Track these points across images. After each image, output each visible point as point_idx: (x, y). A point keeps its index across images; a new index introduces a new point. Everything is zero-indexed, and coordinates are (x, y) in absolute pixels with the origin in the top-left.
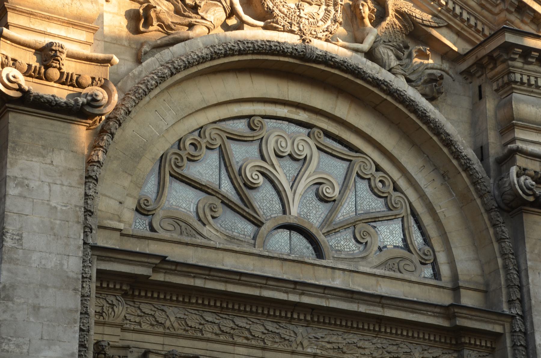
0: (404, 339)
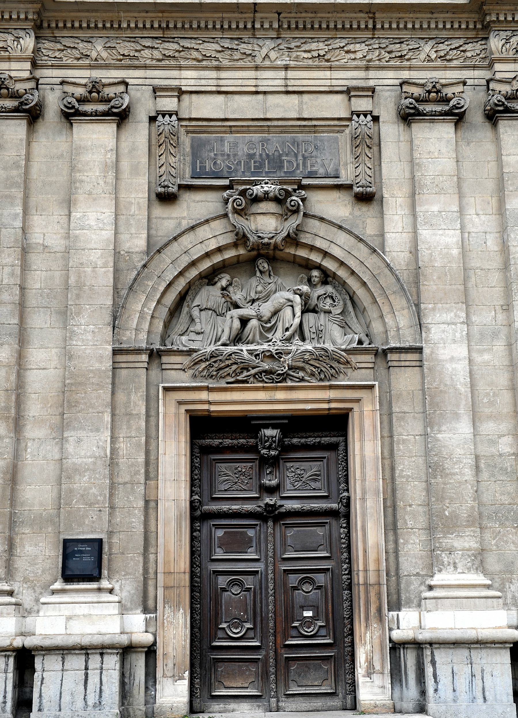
0: (411, 35)
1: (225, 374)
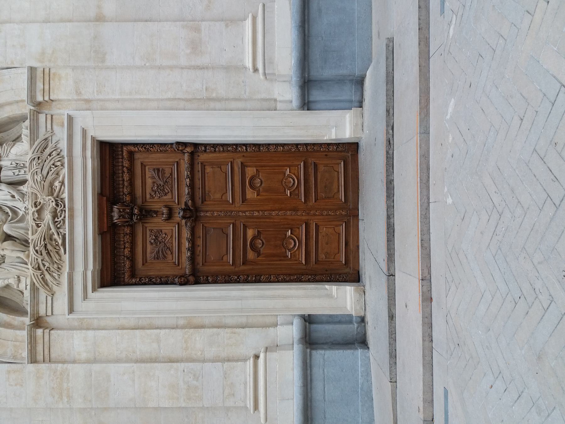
1: (57, 255)
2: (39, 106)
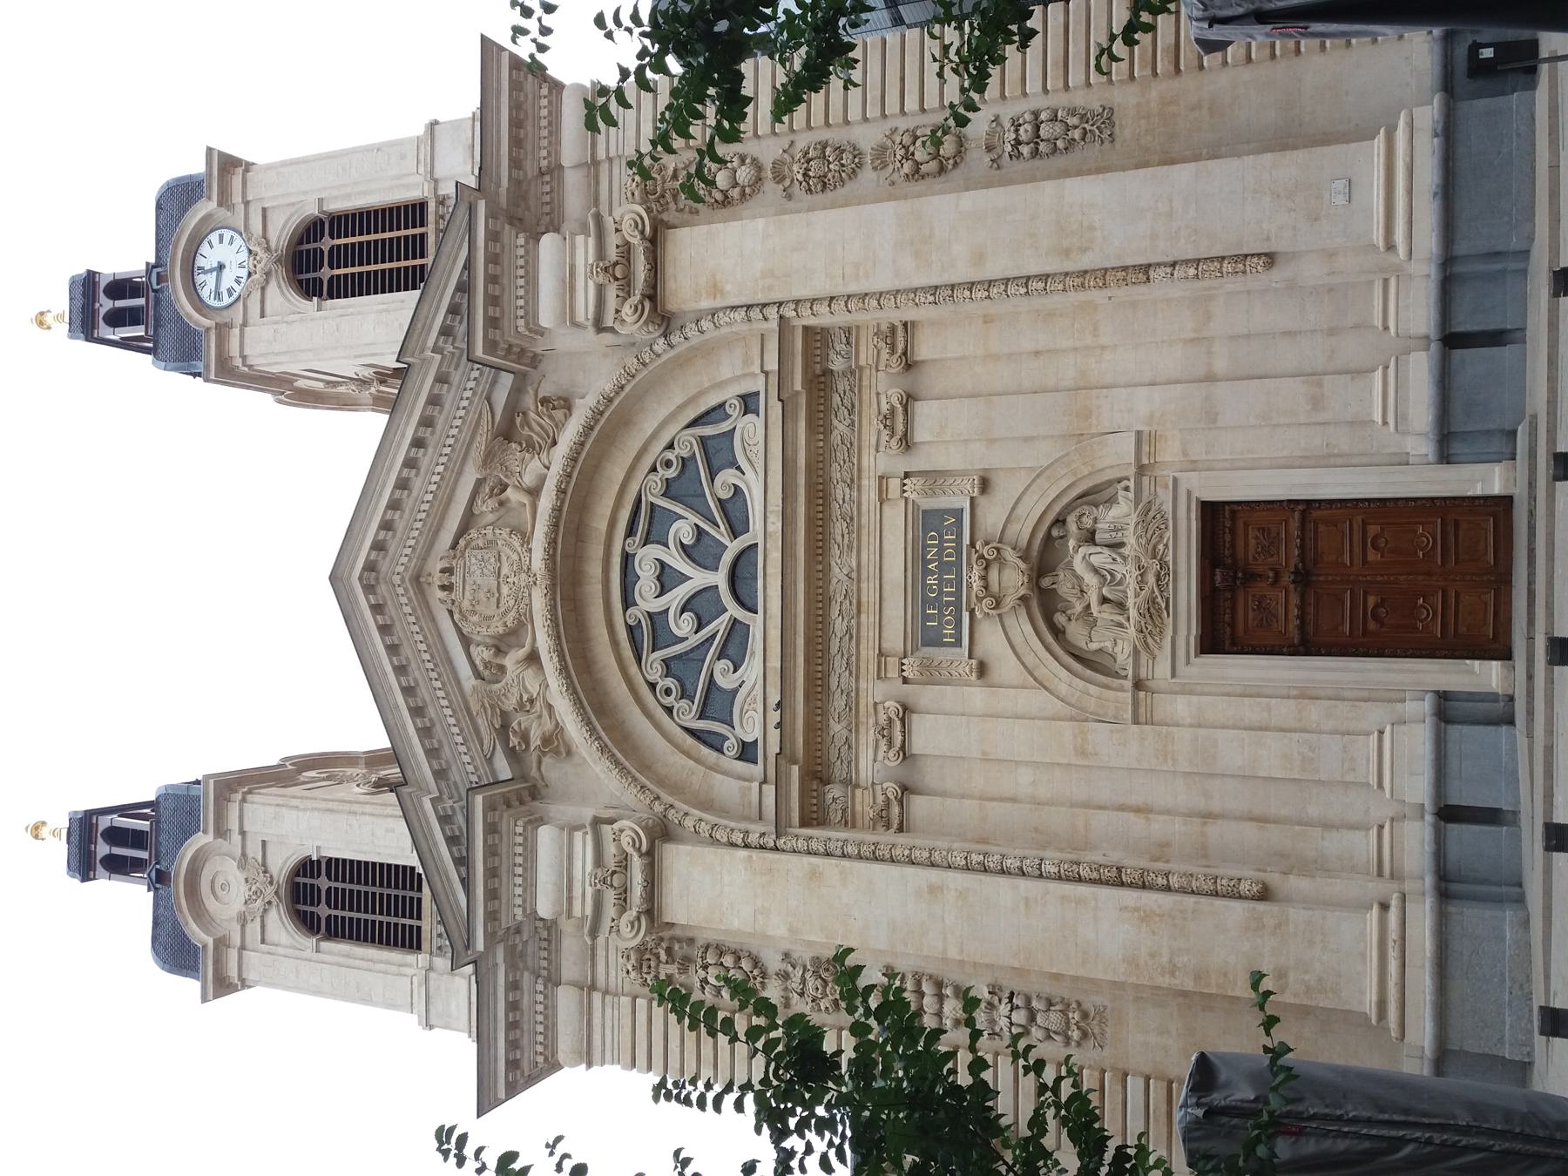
2: (1141, 470)
